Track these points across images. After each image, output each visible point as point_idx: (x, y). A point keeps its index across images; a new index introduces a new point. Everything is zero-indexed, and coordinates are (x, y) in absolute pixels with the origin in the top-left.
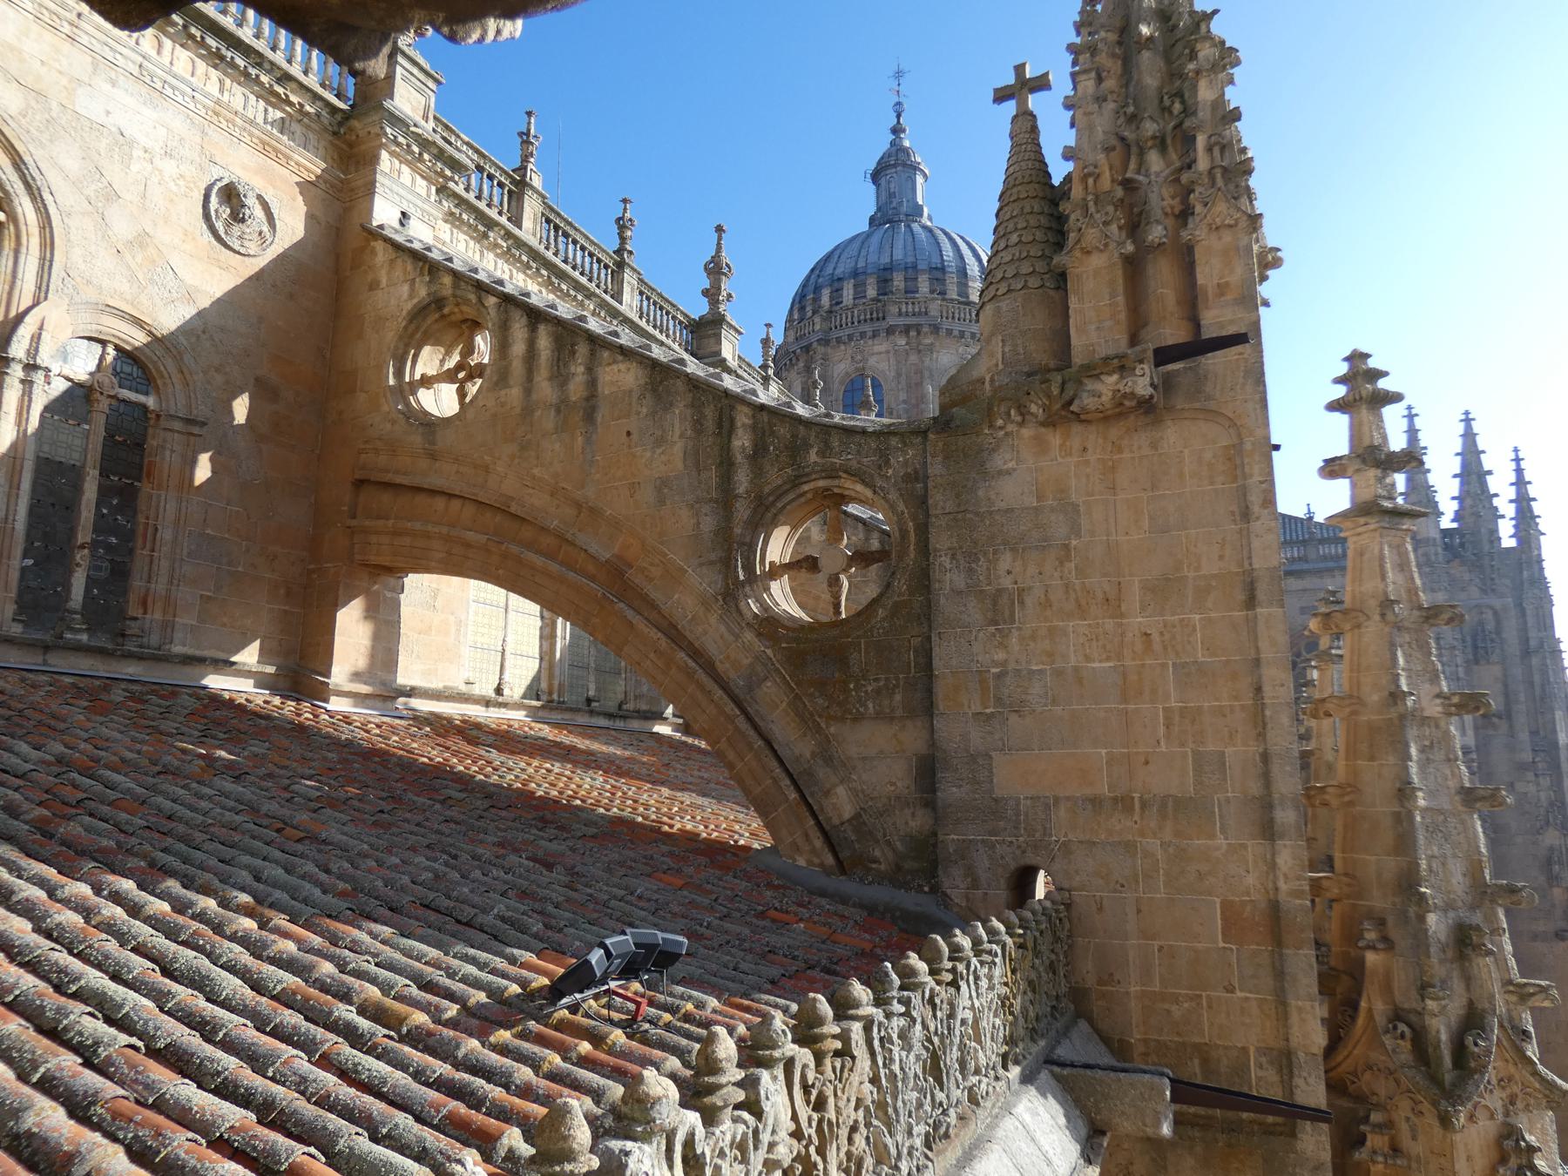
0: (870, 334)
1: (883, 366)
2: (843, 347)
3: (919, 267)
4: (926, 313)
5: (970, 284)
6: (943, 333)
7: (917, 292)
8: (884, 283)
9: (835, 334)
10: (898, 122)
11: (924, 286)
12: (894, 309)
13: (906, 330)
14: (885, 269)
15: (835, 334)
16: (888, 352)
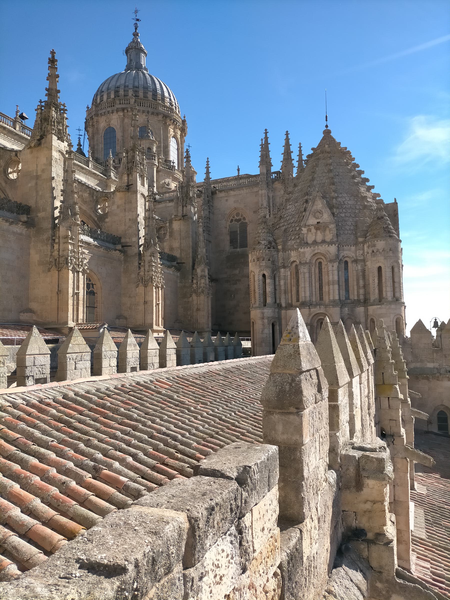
4: (129, 103)
8: (117, 92)
9: (100, 112)
11: (131, 93)
12: (118, 102)
13: (123, 110)
15: (100, 112)
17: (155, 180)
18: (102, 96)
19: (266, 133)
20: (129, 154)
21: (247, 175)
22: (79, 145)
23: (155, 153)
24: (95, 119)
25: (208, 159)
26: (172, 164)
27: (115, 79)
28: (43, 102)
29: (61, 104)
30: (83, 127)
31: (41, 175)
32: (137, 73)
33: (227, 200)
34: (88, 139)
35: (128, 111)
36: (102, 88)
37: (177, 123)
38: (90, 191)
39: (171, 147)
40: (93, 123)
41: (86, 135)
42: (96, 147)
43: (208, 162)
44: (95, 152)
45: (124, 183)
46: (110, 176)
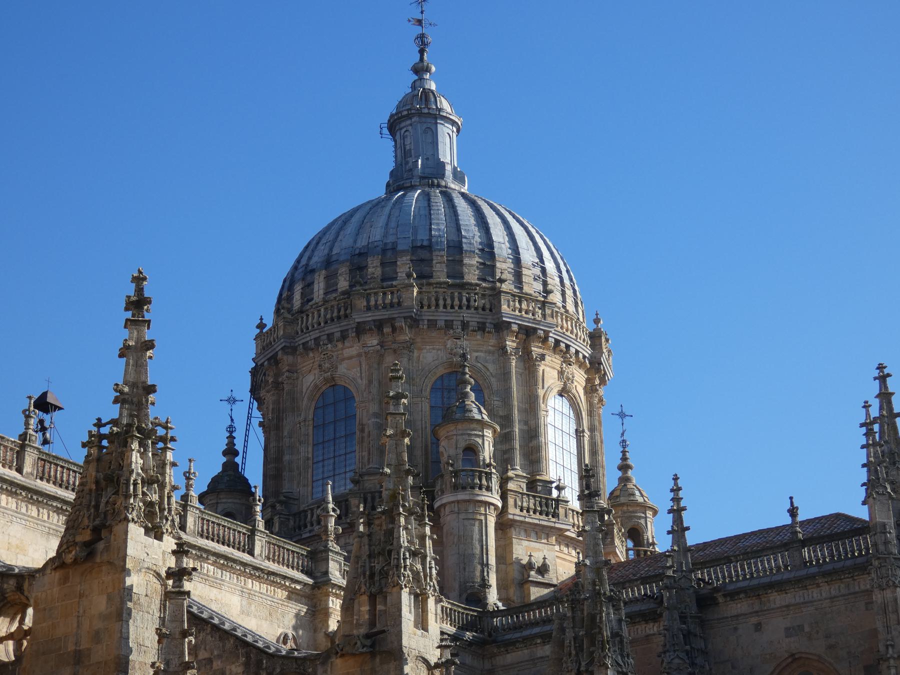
0: (337, 335)
1: (355, 372)
2: (311, 355)
3: (400, 248)
5: (466, 261)
6: (424, 325)
7: (395, 279)
8: (358, 267)
9: (300, 340)
10: (422, 59)
12: (361, 303)
14: (360, 254)
16: (359, 355)
17: (492, 560)
18: (309, 285)
19: (883, 379)
20: (375, 528)
21: (838, 516)
22: (230, 451)
23: (489, 465)
24: (287, 360)
25: (676, 478)
26: (555, 494)
27: (351, 228)
28: (105, 425)
29: (160, 425)
30: (246, 382)
31: (89, 649)
32: (427, 197)
33: (758, 627)
34: (261, 424)
35: (394, 329)
36: (310, 258)
37: (568, 346)
38: (248, 657)
39: (550, 430)
40: (277, 375)
41: (256, 413)
42: (286, 458)
43: (676, 490)
44: (286, 474)
45: (359, 625)
46: (326, 573)
